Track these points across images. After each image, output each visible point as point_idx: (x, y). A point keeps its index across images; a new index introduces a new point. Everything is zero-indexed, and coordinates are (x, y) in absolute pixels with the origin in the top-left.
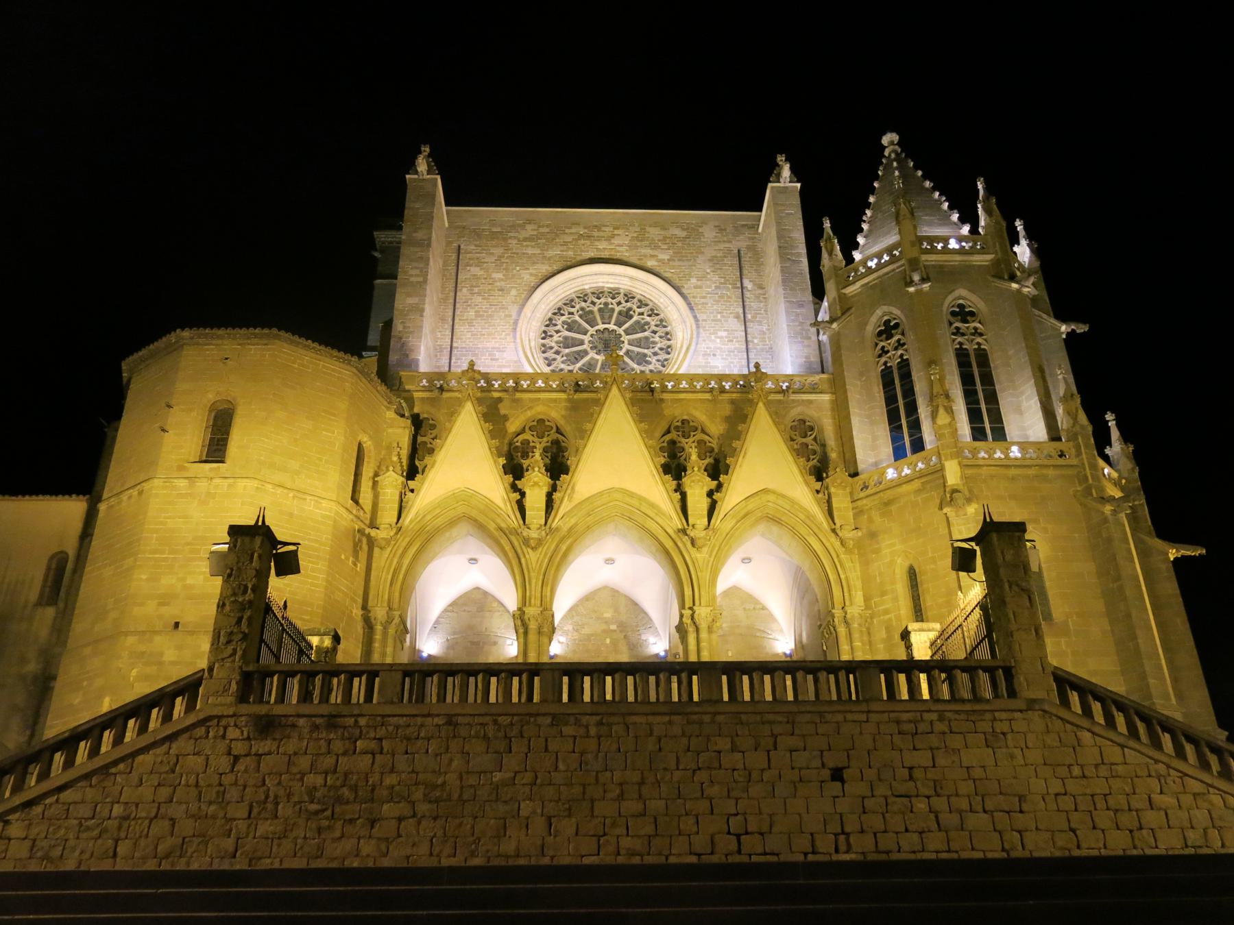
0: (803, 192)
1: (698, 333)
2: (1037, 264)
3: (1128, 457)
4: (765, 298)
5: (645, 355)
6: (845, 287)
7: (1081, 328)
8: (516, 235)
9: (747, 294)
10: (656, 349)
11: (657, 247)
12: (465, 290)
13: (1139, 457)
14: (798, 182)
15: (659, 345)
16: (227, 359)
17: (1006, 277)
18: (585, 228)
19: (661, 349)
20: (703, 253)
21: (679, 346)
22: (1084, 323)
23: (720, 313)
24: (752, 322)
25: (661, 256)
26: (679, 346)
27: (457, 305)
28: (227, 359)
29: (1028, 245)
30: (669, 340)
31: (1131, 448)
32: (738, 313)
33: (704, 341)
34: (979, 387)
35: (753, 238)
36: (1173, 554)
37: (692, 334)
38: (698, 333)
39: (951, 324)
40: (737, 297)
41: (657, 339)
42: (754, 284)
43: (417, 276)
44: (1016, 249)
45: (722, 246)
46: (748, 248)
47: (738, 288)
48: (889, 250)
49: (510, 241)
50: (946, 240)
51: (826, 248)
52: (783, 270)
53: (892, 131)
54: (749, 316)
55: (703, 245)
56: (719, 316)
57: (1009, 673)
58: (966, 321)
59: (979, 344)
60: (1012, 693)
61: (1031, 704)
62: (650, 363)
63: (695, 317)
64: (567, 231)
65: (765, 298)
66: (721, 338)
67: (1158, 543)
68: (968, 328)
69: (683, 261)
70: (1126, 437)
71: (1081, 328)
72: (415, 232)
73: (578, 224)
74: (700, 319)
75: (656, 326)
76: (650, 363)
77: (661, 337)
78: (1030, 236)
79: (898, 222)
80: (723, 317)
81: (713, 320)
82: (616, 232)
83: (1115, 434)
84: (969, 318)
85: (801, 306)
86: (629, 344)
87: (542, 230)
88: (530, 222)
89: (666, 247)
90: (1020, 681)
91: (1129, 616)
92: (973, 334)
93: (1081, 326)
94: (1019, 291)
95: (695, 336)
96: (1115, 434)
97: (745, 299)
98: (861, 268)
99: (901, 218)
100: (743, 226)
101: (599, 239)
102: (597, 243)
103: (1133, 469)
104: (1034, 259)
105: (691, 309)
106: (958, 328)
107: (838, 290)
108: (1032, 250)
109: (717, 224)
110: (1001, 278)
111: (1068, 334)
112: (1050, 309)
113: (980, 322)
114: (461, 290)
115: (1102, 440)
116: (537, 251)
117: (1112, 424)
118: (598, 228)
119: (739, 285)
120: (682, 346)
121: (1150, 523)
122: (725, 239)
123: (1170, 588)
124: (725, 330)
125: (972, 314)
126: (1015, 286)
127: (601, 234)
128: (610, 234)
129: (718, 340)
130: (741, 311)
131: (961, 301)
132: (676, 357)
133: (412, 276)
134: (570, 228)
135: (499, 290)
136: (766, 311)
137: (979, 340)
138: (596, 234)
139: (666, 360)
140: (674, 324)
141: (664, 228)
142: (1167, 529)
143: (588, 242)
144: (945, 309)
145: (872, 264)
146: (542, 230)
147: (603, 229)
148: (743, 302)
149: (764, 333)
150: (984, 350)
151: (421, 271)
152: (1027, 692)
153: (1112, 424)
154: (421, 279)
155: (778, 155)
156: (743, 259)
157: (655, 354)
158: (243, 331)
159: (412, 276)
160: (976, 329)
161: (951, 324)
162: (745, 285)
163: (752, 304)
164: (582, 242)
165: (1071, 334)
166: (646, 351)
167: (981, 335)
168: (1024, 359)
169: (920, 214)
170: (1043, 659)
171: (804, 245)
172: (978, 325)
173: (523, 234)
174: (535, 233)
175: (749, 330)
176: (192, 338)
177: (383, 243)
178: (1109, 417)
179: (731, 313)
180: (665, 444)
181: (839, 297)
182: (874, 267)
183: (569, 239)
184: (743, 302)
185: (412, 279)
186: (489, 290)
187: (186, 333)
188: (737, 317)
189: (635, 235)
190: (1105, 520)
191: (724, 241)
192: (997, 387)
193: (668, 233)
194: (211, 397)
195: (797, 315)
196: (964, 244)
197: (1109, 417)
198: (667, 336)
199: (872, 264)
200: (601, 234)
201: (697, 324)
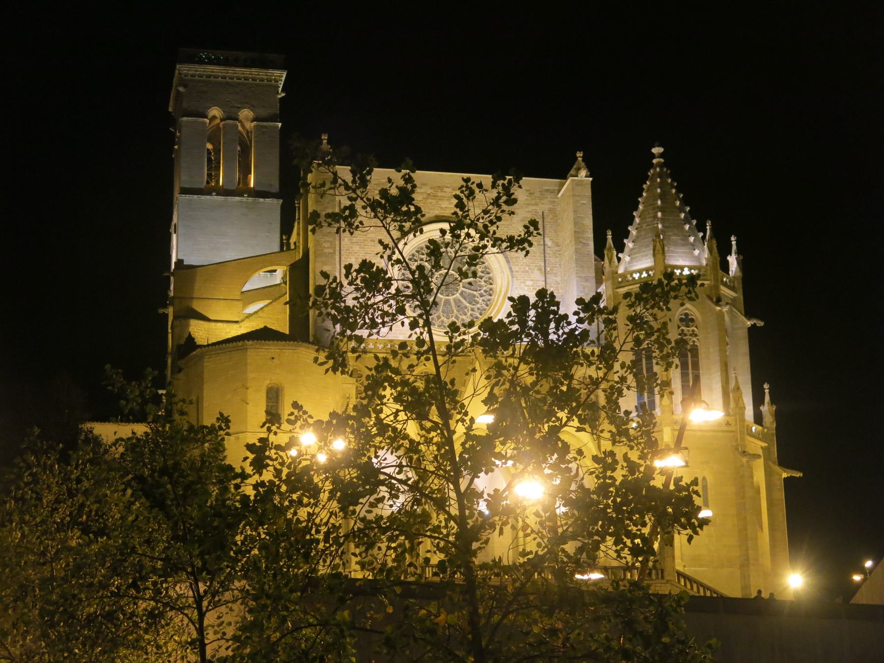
0: (592, 182)
1: (513, 282)
2: (740, 274)
3: (771, 415)
4: (560, 254)
5: (474, 296)
6: (617, 288)
7: (760, 324)
9: (548, 251)
10: (482, 291)
13: (778, 416)
14: (590, 177)
15: (484, 288)
16: (273, 358)
17: (714, 300)
18: (431, 188)
19: (485, 291)
21: (498, 290)
22: (762, 320)
23: (528, 266)
24: (551, 274)
26: (498, 290)
27: (342, 252)
28: (273, 358)
29: (736, 259)
30: (491, 284)
31: (774, 408)
32: (540, 266)
33: (516, 288)
34: (690, 371)
35: (554, 202)
36: (785, 475)
37: (508, 282)
38: (513, 282)
39: (679, 327)
40: (541, 253)
41: (483, 283)
42: (553, 242)
44: (729, 258)
45: (531, 208)
46: (550, 210)
47: (541, 245)
48: (647, 270)
50: (682, 269)
51: (608, 255)
52: (577, 251)
53: (659, 146)
54: (548, 269)
56: (527, 268)
57: (662, 571)
58: (688, 326)
59: (694, 342)
60: (663, 578)
61: (668, 581)
62: (478, 303)
63: (510, 268)
65: (560, 254)
66: (528, 286)
67: (777, 469)
68: (688, 330)
70: (773, 401)
71: (760, 324)
73: (425, 184)
74: (514, 270)
75: (482, 272)
76: (478, 303)
77: (485, 282)
78: (738, 252)
79: (654, 255)
80: (531, 269)
81: (523, 272)
83: (767, 398)
84: (690, 323)
85: (587, 280)
86: (463, 287)
90: (666, 574)
91: (745, 518)
92: (691, 335)
93: (760, 322)
94: (720, 311)
95: (510, 283)
96: (767, 398)
97: (546, 255)
98: (629, 276)
99: (656, 253)
100: (547, 190)
102: (440, 202)
103: (773, 422)
104: (738, 270)
105: (508, 262)
106: (683, 330)
107: (613, 289)
108: (738, 263)
109: (528, 189)
110: (711, 299)
111: (752, 325)
112: (743, 308)
113: (696, 327)
114: (344, 240)
115: (758, 401)
117: (767, 391)
118: (441, 188)
119: (542, 243)
120: (500, 292)
121: (776, 456)
122: (533, 202)
123: (780, 495)
124: (531, 280)
125: (692, 320)
126: (718, 308)
127: (444, 194)
129: (526, 288)
130: (543, 264)
131: (687, 311)
132: (496, 299)
133: (325, 247)
135: (371, 241)
136: (560, 265)
137: (694, 339)
138: (440, 194)
139: (489, 300)
140: (495, 272)
142: (784, 462)
143: (434, 201)
144: (676, 317)
145: (636, 276)
147: (445, 189)
148: (545, 257)
149: (559, 284)
150: (697, 346)
151: (331, 244)
152: (667, 578)
153: (767, 391)
154: (331, 251)
155: (578, 152)
156: (545, 220)
157: (482, 296)
158: (284, 343)
160: (693, 331)
161: (679, 327)
162: (546, 243)
163: (551, 259)
164: (430, 201)
165: (754, 326)
166: (475, 293)
167: (696, 335)
168: (718, 358)
169: (670, 234)
170: (674, 567)
171: (592, 230)
172: (695, 329)
175: (548, 280)
176: (252, 345)
177: (186, 75)
178: (766, 386)
179: (536, 266)
180: (502, 392)
181: (614, 294)
182: (637, 278)
184: (545, 257)
186: (364, 240)
187: (250, 342)
188: (540, 270)
190: (742, 466)
191: (532, 204)
192: (701, 372)
194: (268, 382)
195: (584, 288)
196: (693, 271)
197: (766, 386)
198: (490, 281)
199: (636, 276)
200: (444, 194)
201: (512, 275)
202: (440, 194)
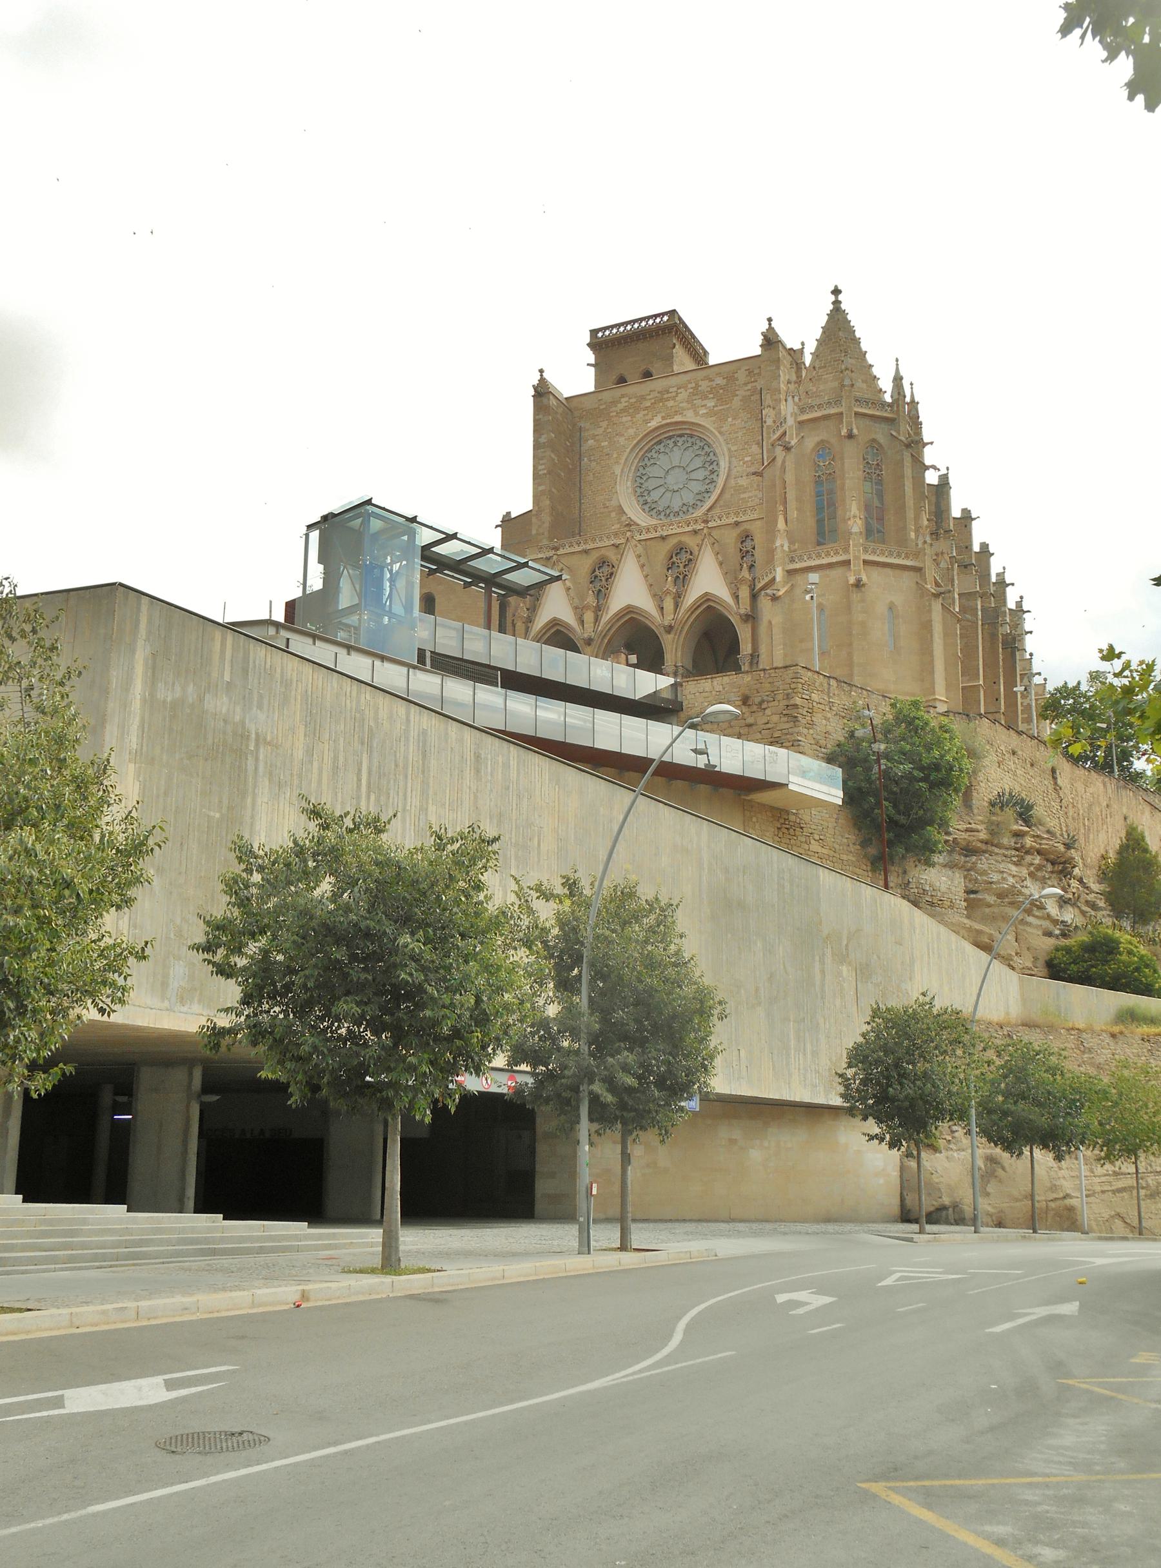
8: (614, 409)
11: (706, 398)
12: (586, 459)
20: (737, 395)
25: (708, 405)
27: (582, 472)
43: (543, 469)
45: (749, 387)
49: (611, 414)
55: (737, 388)
64: (648, 397)
69: (722, 405)
72: (540, 437)
82: (679, 391)
87: (631, 401)
88: (623, 396)
89: (712, 396)
101: (668, 400)
116: (629, 418)
128: (674, 394)
130: (761, 438)
134: (650, 394)
135: (608, 454)
141: (711, 380)
143: (661, 404)
146: (631, 401)
159: (540, 470)
173: (620, 406)
174: (627, 404)
183: (648, 404)
185: (540, 473)
188: (758, 444)
189: (692, 390)
193: (714, 384)
200: (669, 395)
202: (665, 396)
